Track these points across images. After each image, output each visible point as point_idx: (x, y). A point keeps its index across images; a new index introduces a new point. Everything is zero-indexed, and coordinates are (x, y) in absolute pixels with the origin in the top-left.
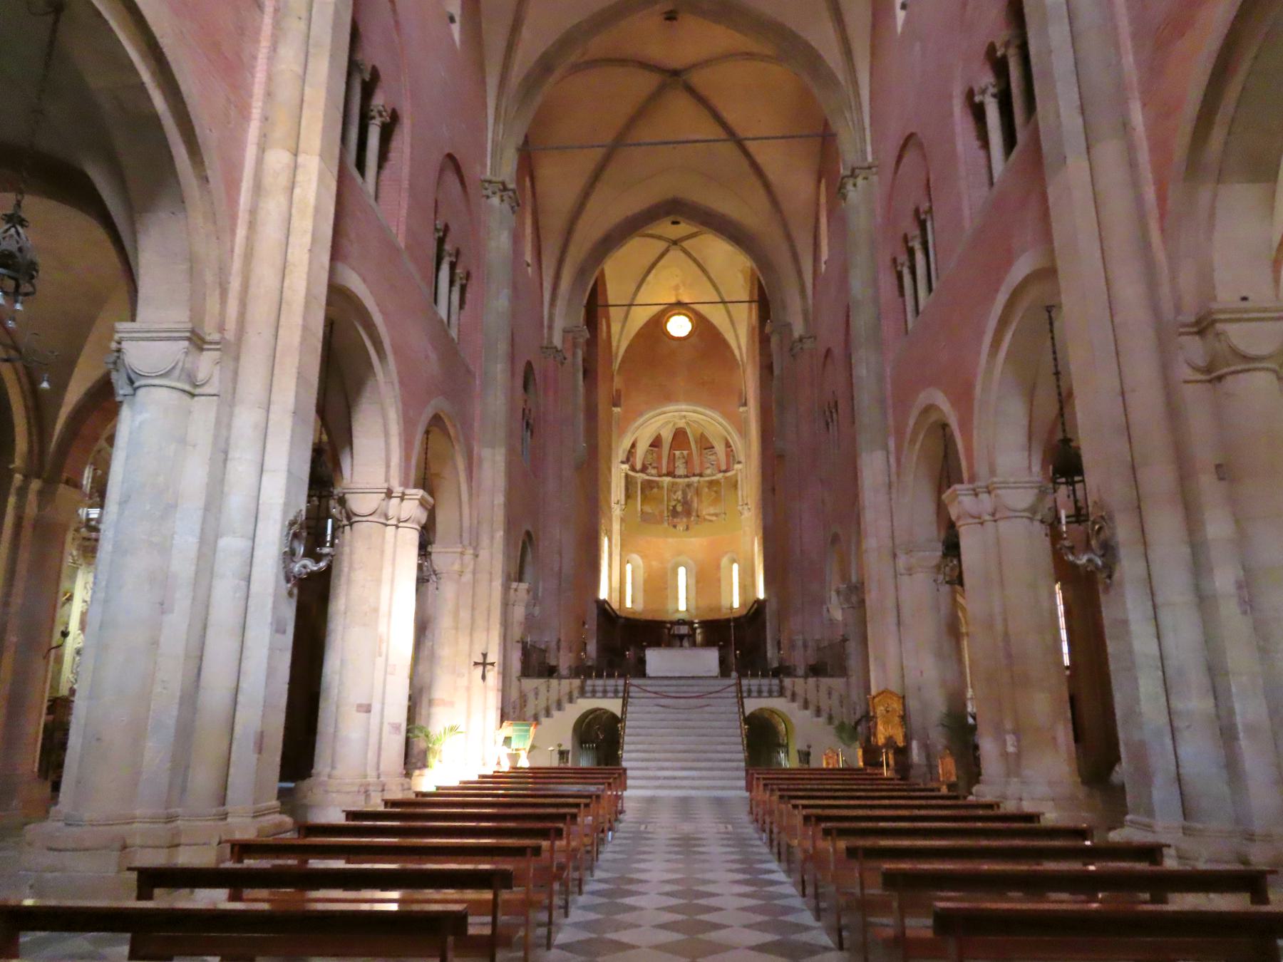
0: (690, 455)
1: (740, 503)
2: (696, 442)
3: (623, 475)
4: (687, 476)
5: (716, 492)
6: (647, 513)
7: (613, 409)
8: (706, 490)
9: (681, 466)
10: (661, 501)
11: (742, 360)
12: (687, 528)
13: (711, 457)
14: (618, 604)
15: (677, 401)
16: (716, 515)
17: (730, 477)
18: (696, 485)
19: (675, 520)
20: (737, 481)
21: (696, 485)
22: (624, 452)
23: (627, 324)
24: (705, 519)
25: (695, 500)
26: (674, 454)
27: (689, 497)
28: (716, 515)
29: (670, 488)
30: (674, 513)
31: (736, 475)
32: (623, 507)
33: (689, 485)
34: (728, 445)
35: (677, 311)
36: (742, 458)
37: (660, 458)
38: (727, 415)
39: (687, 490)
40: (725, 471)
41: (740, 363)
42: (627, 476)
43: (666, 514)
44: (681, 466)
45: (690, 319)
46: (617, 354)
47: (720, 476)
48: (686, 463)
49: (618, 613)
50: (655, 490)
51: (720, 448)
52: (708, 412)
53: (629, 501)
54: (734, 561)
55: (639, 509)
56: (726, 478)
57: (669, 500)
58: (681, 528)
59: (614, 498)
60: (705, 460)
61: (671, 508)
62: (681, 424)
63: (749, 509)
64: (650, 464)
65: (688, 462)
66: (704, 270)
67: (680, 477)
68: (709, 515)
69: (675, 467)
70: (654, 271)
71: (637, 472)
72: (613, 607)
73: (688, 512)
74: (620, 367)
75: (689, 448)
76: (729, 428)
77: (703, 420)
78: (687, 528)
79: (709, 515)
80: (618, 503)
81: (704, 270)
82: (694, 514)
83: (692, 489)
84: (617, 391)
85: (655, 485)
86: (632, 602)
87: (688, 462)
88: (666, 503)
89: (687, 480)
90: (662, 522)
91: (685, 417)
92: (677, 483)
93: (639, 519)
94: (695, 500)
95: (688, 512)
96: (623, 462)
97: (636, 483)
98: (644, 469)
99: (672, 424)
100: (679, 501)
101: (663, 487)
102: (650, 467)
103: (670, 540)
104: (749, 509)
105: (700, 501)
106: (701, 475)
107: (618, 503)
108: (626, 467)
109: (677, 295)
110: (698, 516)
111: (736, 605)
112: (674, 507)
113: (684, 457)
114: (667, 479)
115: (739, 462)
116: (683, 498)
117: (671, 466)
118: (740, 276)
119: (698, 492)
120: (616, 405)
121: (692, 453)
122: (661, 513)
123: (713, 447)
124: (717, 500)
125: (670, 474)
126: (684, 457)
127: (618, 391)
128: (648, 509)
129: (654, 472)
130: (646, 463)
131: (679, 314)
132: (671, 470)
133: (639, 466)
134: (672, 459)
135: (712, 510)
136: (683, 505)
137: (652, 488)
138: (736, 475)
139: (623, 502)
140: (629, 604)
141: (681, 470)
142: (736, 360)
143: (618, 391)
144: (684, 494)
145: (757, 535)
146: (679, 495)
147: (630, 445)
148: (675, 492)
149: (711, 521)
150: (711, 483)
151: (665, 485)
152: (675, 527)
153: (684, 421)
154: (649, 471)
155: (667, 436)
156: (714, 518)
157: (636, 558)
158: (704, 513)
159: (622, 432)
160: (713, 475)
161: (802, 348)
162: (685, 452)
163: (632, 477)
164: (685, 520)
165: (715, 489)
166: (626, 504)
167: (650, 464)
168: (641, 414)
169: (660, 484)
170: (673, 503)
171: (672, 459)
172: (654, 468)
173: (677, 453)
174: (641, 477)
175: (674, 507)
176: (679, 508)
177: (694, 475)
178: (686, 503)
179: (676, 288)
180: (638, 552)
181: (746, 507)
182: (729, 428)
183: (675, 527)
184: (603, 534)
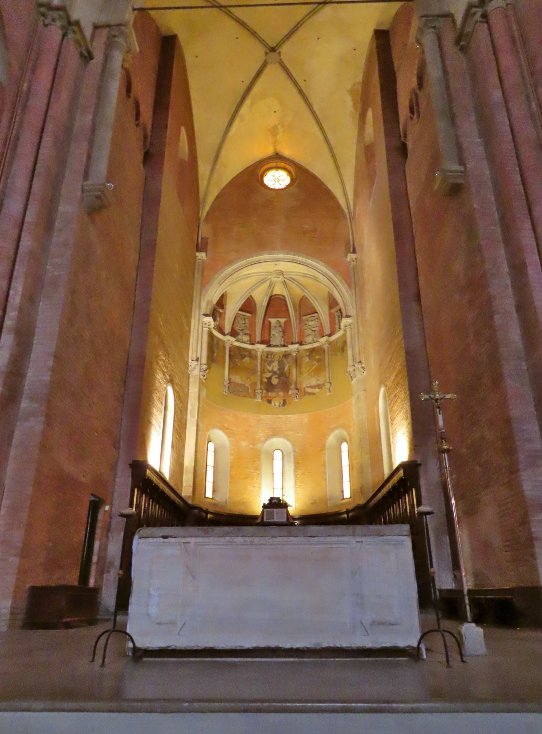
0: (288, 323)
1: (350, 363)
2: (295, 309)
3: (206, 330)
4: (284, 346)
5: (318, 361)
6: (236, 384)
7: (198, 254)
8: (307, 360)
9: (277, 335)
10: (253, 371)
11: (348, 208)
12: (284, 403)
13: (310, 323)
14: (191, 489)
15: (272, 249)
16: (319, 386)
17: (337, 341)
18: (294, 354)
19: (270, 394)
20: (345, 343)
21: (294, 354)
22: (208, 302)
23: (217, 167)
24: (306, 393)
25: (294, 371)
26: (270, 323)
27: (286, 369)
28: (319, 386)
29: (264, 358)
30: (269, 386)
31: (344, 335)
32: (205, 367)
33: (286, 355)
34: (332, 303)
35: (274, 165)
36: (352, 311)
37: (252, 325)
38: (335, 266)
39: (284, 360)
40: (330, 335)
41: (346, 211)
42: (211, 336)
43: (259, 386)
44: (277, 335)
45: (289, 173)
46: (204, 200)
47: (323, 340)
48: (284, 332)
49: (190, 502)
50: (247, 360)
51: (323, 311)
52: (309, 261)
53: (214, 366)
54: (344, 440)
55: (226, 377)
56: (330, 343)
57: (263, 372)
58: (276, 403)
59: (192, 354)
60: (305, 327)
61: (266, 380)
62: (279, 290)
63: (363, 368)
64: (242, 330)
65: (286, 330)
66: (306, 99)
67: (276, 346)
68: (311, 387)
69: (270, 337)
70: (248, 102)
71: (223, 334)
72: (183, 495)
73: (285, 385)
74: (208, 214)
75: (287, 315)
76: (335, 279)
77: (305, 275)
78: (284, 403)
79: (311, 387)
80: (197, 360)
81: (306, 99)
82: (293, 387)
83: (290, 359)
84: (202, 238)
85: (246, 354)
86: (214, 491)
87: (286, 330)
88: (259, 373)
89: (284, 349)
90: (255, 396)
91: (282, 273)
92: (272, 353)
93: (227, 389)
94: (294, 371)
95: (285, 385)
96: (206, 315)
97: (224, 347)
98: (234, 333)
99: (267, 283)
100: (274, 373)
101: (256, 357)
102: (241, 333)
103: (262, 417)
104: (363, 368)
105: (301, 373)
106: (301, 344)
107: (197, 360)
108: (210, 319)
109: (275, 143)
110: (297, 389)
111: (347, 494)
112: (269, 379)
113: (281, 326)
114: (262, 347)
115: (348, 316)
116: (279, 369)
117: (266, 335)
118: (348, 98)
119: (297, 361)
120: (198, 250)
121: (290, 320)
122: (255, 384)
123: (316, 312)
124: (319, 370)
125: (266, 342)
126: (281, 326)
127: (205, 241)
128: (237, 379)
129: (246, 338)
130: (237, 328)
131: (277, 168)
132: (266, 339)
133: (227, 329)
134: (267, 327)
135: (314, 382)
136: (279, 378)
137: (243, 357)
138: (344, 335)
139: (204, 360)
140: (209, 494)
141: (277, 337)
142: (342, 210)
143: (205, 241)
144: (281, 363)
145: (382, 382)
146: (275, 366)
147: (215, 301)
148: (270, 365)
149: (313, 394)
150: (312, 351)
151: (259, 354)
152: (270, 402)
153: (281, 279)
154: (240, 337)
155: (261, 301)
156: (316, 390)
157: (218, 435)
158: (304, 386)
159: (205, 284)
160: (314, 342)
161: (485, 16)
162: (283, 320)
163: (219, 340)
164: (281, 394)
165: (317, 357)
166: (209, 368)
167: (242, 330)
168: (230, 262)
169: (253, 352)
170: (269, 375)
171: (267, 327)
172: (246, 334)
173: (273, 321)
174: (229, 340)
175: (269, 379)
176: (275, 381)
177: (292, 343)
178: (283, 375)
179: (274, 131)
180: (223, 428)
181: (358, 366)
182: (335, 279)
183: (270, 402)
184: (159, 376)
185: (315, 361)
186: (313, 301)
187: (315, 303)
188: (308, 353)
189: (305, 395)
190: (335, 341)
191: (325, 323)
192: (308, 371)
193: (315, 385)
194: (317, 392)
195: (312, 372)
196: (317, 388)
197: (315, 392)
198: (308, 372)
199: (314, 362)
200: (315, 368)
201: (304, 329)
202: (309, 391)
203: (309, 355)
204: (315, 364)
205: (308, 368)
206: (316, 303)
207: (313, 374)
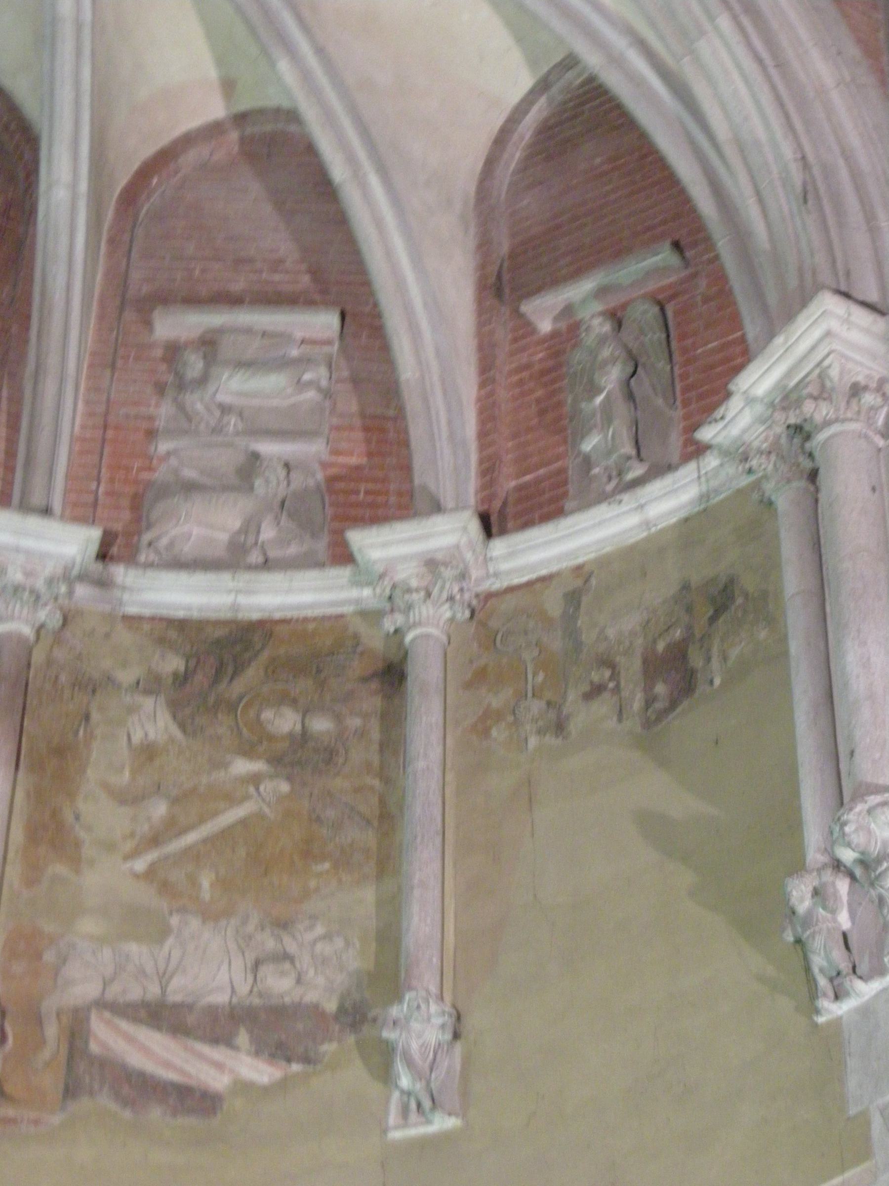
185: (248, 752)
186: (351, 159)
187: (364, 186)
188: (174, 663)
189: (70, 1091)
190: (553, 604)
191: (438, 401)
192: (155, 840)
193: (221, 998)
194: (243, 1087)
195: (193, 855)
196: (243, 1038)
197: (218, 1082)
198: (151, 856)
199: (242, 766)
200: (243, 822)
201: (151, 434)
202: (136, 1060)
203: (182, 680)
204: (255, 779)
205: (160, 809)
206: (374, 181)
207: (206, 881)
